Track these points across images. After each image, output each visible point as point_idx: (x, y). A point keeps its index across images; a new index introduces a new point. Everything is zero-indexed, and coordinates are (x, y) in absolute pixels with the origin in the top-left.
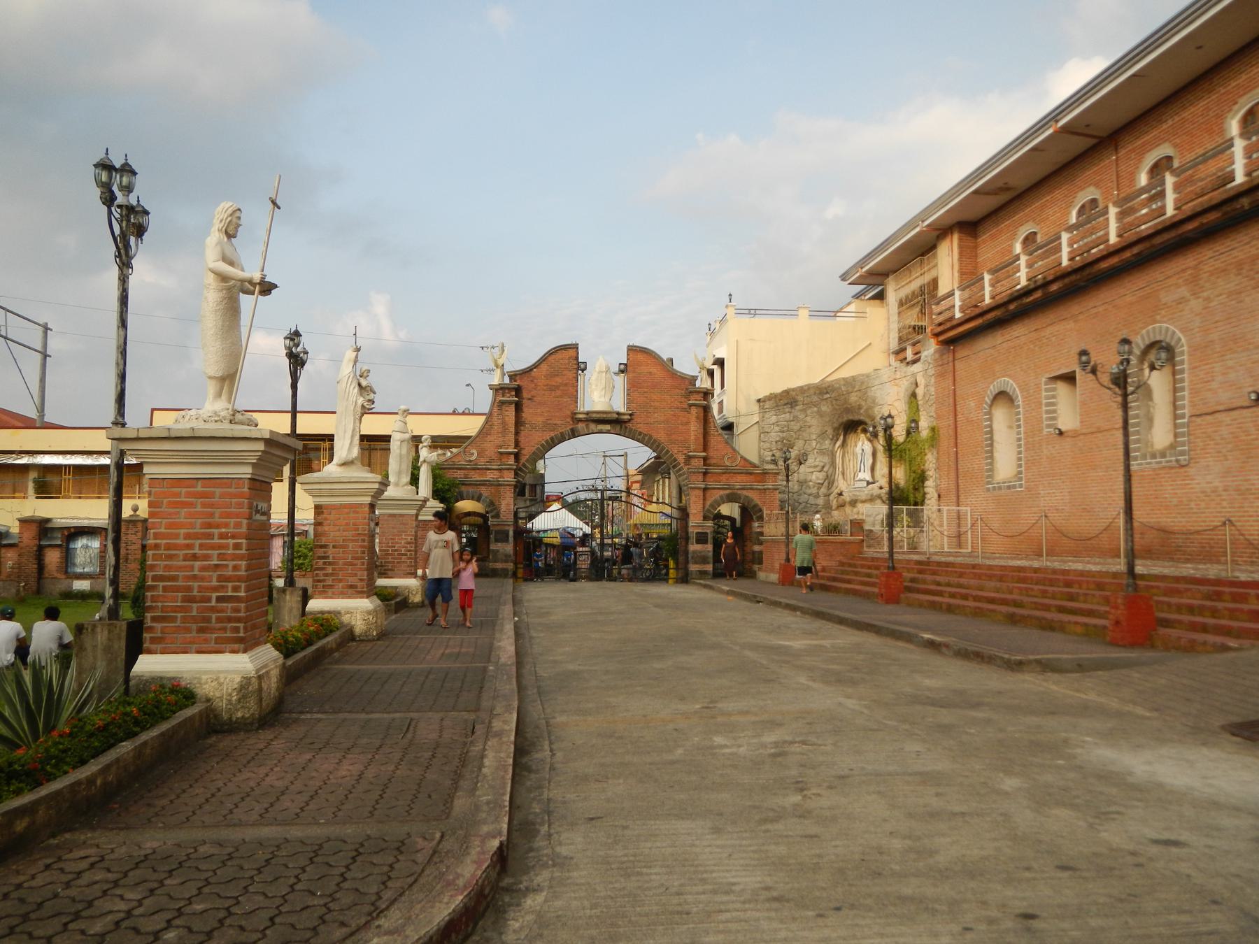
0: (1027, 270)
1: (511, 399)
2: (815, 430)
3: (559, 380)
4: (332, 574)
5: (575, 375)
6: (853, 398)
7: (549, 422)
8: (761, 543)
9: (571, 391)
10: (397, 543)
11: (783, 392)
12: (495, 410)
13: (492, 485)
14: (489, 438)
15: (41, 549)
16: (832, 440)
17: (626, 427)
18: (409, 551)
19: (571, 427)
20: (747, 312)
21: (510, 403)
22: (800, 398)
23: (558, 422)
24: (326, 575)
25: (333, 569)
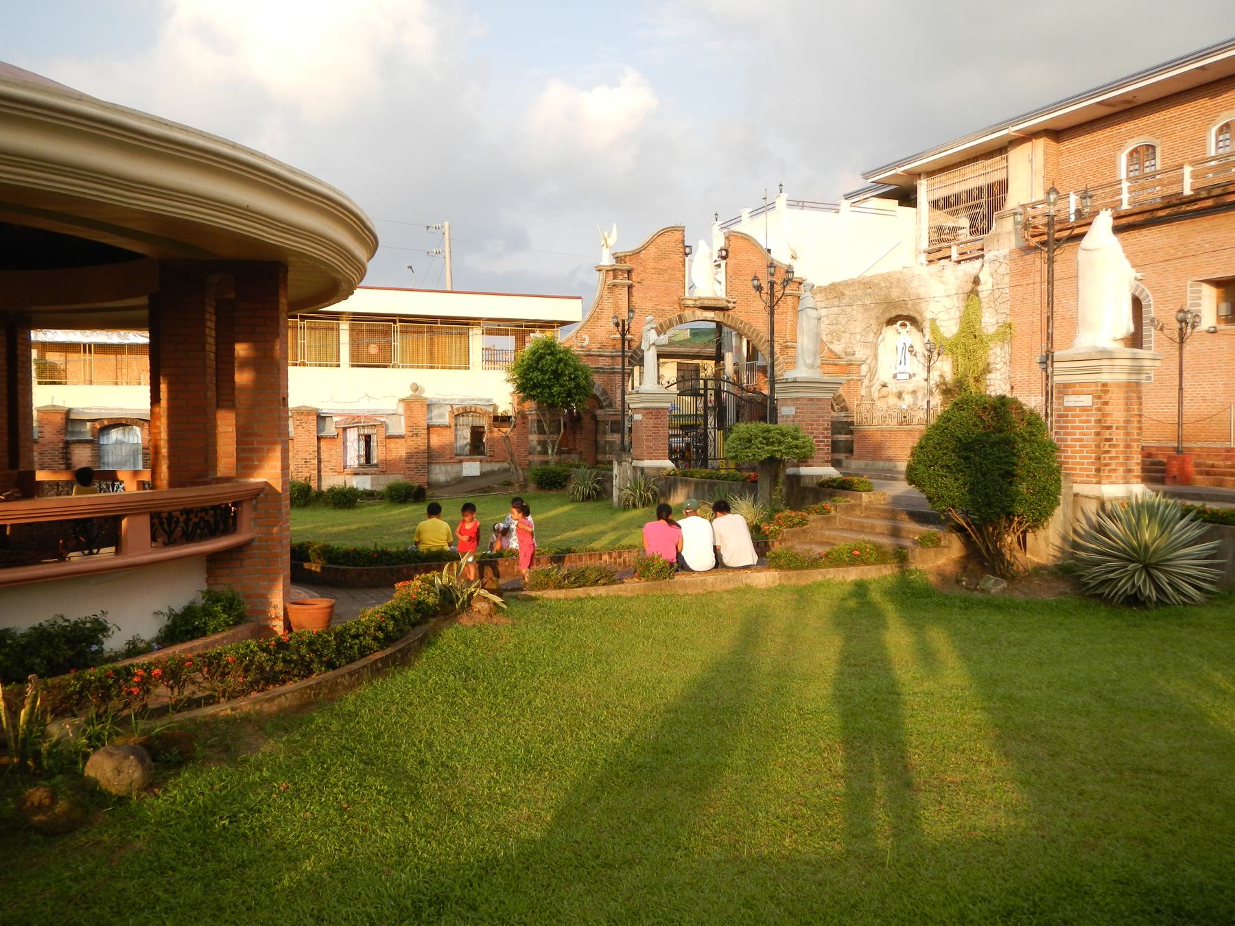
0: (1192, 180)
1: (624, 281)
2: (858, 326)
3: (666, 263)
4: (1116, 458)
5: (681, 259)
6: (895, 294)
7: (658, 307)
8: (851, 432)
9: (678, 274)
10: (816, 429)
11: (830, 285)
12: (606, 292)
13: (604, 373)
14: (600, 322)
15: (67, 444)
16: (875, 333)
17: (729, 316)
18: (827, 437)
19: (679, 313)
20: (795, 203)
21: (623, 285)
22: (846, 292)
23: (667, 308)
24: (1111, 458)
25: (1117, 453)
